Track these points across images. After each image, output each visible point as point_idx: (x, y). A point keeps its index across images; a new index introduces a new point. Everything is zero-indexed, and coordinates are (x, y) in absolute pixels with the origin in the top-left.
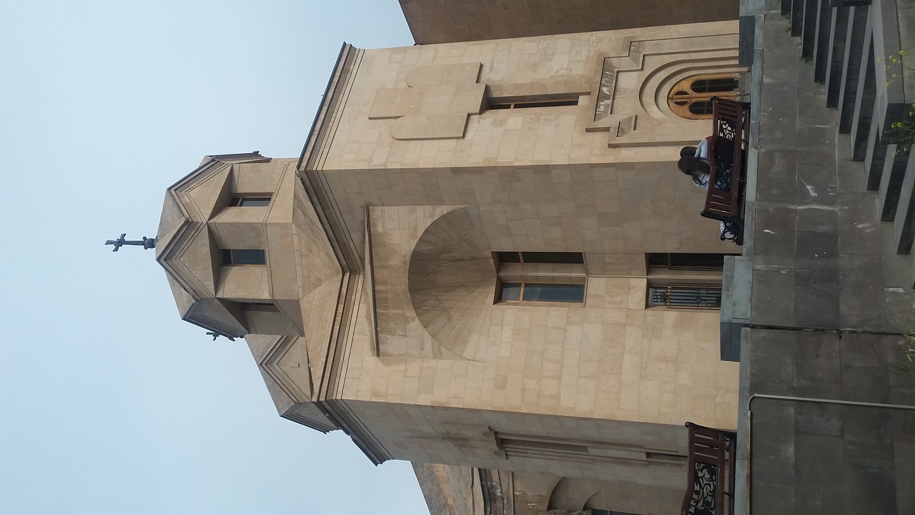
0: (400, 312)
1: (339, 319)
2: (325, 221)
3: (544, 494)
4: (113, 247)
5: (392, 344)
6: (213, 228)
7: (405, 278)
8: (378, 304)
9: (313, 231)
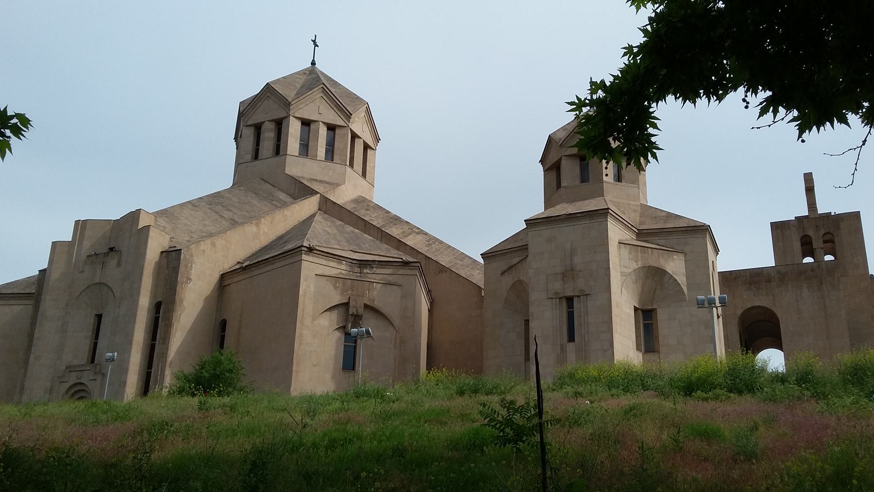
0: (640, 259)
2: (675, 230)
3: (376, 303)
5: (625, 251)
7: (655, 265)
9: (655, 217)
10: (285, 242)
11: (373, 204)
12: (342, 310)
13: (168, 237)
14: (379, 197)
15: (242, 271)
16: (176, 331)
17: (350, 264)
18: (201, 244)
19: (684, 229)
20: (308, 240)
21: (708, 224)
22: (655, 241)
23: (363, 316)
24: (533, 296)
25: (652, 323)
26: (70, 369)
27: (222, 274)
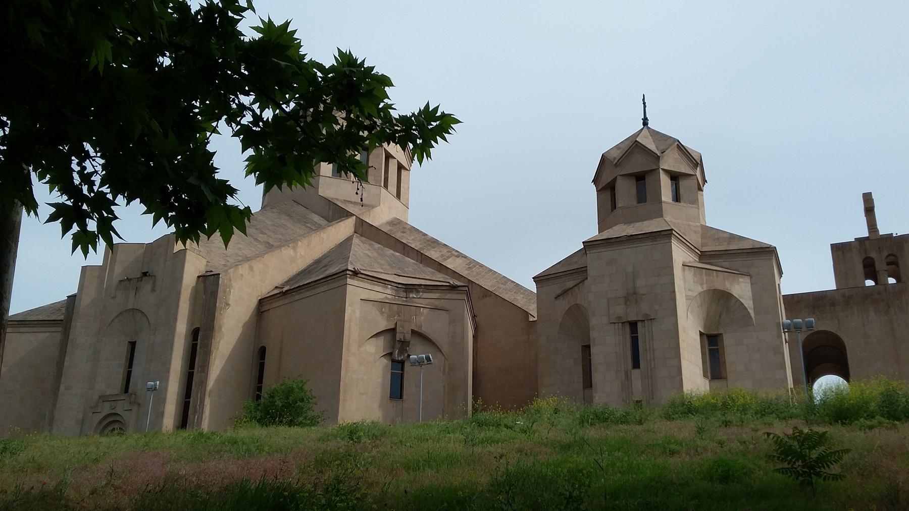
2: (740, 251)
5: (690, 273)
6: (692, 178)
7: (721, 288)
9: (718, 239)
10: (326, 266)
11: (409, 227)
12: (389, 336)
13: (204, 262)
14: (413, 219)
15: (281, 296)
16: (215, 358)
17: (396, 288)
18: (238, 269)
19: (749, 251)
20: (352, 264)
21: (774, 245)
22: (716, 263)
23: (411, 342)
24: (594, 321)
25: (718, 349)
26: (103, 398)
27: (260, 300)
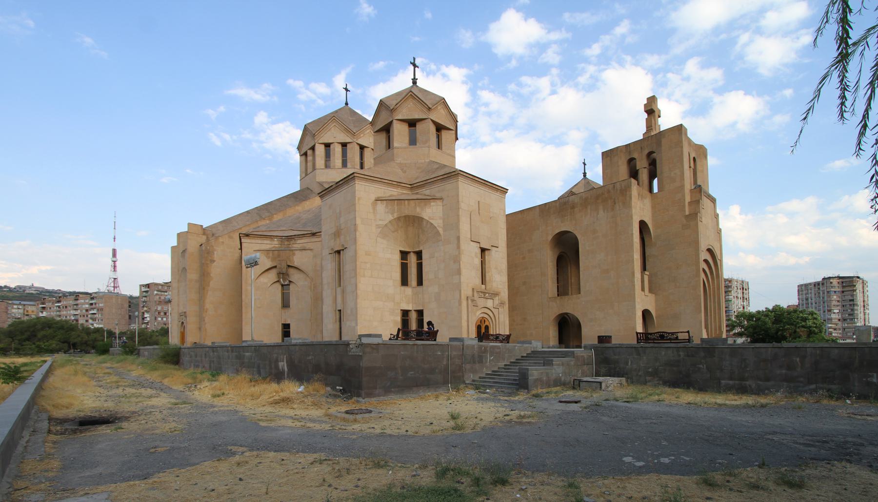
0: (396, 211)
1: (390, 182)
3: (295, 263)
4: (412, 61)
5: (381, 207)
6: (426, 121)
8: (399, 201)
9: (428, 171)
